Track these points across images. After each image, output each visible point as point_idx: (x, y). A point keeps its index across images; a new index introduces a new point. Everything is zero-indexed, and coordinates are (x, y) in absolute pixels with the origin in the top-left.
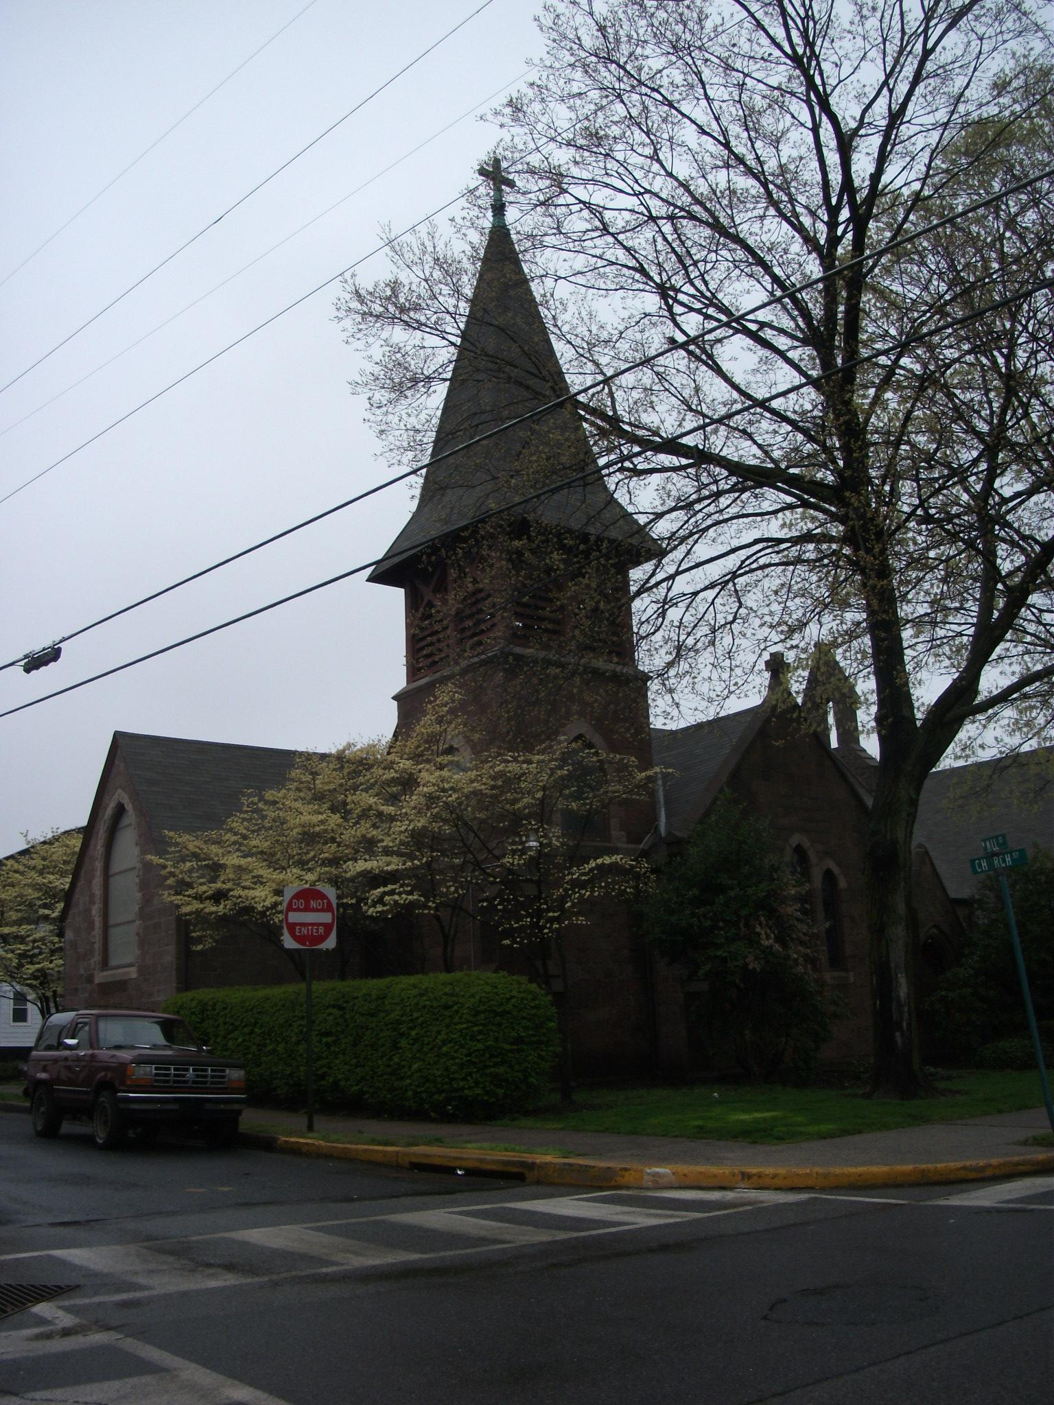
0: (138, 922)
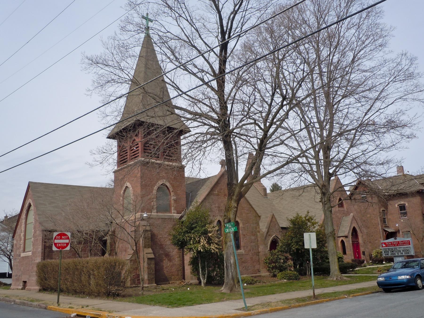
0: (33, 239)
